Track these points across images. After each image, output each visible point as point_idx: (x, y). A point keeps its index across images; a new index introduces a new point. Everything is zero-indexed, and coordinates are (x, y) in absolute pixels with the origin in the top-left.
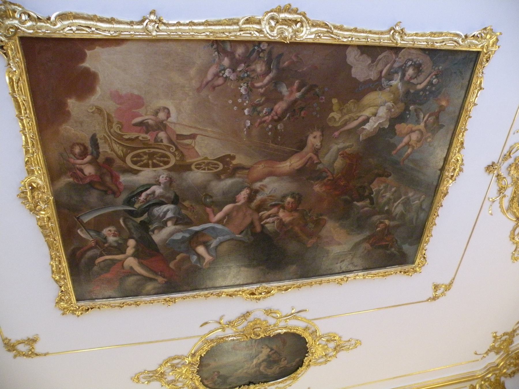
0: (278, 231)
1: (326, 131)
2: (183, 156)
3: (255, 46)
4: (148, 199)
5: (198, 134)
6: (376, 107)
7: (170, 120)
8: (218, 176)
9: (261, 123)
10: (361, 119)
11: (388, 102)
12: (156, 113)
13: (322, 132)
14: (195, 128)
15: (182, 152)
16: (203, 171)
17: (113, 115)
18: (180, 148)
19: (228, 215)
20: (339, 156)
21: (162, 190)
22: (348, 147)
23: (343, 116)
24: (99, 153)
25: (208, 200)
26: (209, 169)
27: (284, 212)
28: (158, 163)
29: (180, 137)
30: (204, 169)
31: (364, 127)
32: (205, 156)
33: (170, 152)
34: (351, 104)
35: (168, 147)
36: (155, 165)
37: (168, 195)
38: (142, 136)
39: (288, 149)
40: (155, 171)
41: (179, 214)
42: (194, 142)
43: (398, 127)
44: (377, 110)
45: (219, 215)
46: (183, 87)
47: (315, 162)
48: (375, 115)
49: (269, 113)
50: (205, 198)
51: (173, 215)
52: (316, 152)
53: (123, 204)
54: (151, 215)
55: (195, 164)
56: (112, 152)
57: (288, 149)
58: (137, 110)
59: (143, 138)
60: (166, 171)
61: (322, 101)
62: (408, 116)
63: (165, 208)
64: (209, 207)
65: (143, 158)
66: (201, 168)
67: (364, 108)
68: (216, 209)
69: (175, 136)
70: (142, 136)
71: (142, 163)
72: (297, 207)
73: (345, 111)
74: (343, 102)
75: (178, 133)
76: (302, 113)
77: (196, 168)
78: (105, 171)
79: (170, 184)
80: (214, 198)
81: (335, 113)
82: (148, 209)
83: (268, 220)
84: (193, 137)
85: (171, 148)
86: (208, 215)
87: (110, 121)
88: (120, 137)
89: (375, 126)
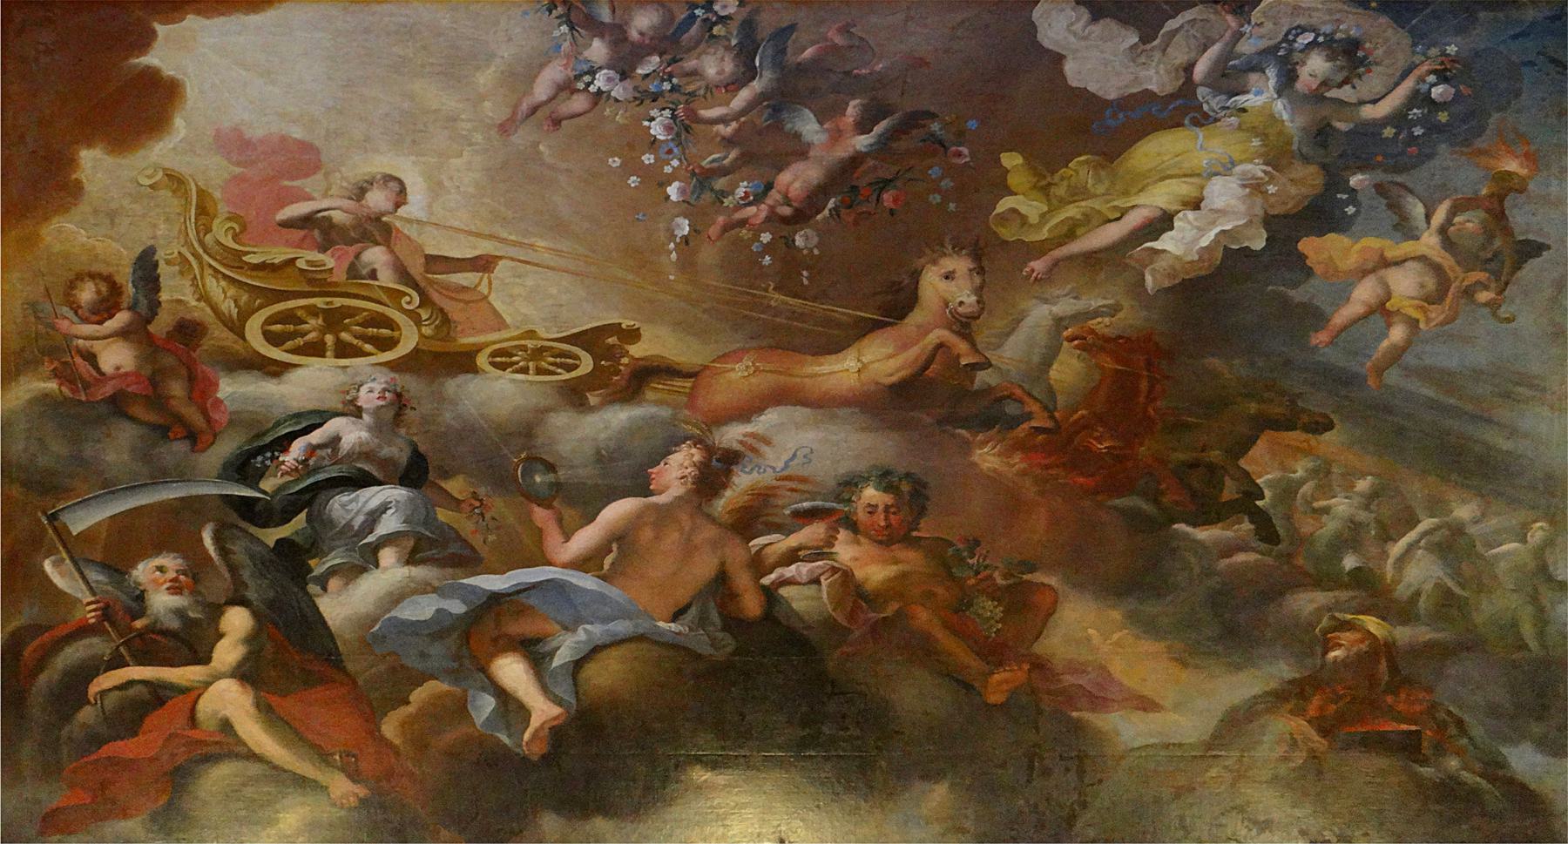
1: (992, 255)
4: (311, 462)
5: (501, 258)
7: (401, 211)
8: (575, 396)
9: (726, 228)
10: (1133, 220)
11: (1241, 162)
12: (360, 192)
13: (977, 256)
14: (491, 237)
15: (441, 310)
17: (217, 194)
18: (435, 297)
19: (621, 538)
21: (364, 435)
22: (1096, 313)
25: (538, 479)
26: (539, 371)
28: (355, 342)
29: (436, 262)
30: (525, 371)
32: (531, 327)
33: (404, 311)
34: (1080, 169)
35: (396, 295)
36: (344, 351)
37: (386, 452)
38: (307, 257)
39: (842, 313)
42: (485, 280)
44: (1202, 188)
45: (586, 538)
47: (964, 362)
48: (1196, 204)
52: (964, 325)
55: (488, 351)
57: (842, 313)
58: (296, 183)
60: (385, 370)
63: (373, 497)
64: (546, 503)
67: (1141, 182)
68: (569, 514)
70: (307, 257)
71: (300, 341)
73: (1061, 191)
74: (1046, 164)
76: (887, 197)
77: (494, 364)
78: (168, 360)
80: (562, 474)
81: (1020, 197)
84: (483, 264)
86: (539, 534)
87: (202, 211)
88: (234, 259)
89: (1204, 242)
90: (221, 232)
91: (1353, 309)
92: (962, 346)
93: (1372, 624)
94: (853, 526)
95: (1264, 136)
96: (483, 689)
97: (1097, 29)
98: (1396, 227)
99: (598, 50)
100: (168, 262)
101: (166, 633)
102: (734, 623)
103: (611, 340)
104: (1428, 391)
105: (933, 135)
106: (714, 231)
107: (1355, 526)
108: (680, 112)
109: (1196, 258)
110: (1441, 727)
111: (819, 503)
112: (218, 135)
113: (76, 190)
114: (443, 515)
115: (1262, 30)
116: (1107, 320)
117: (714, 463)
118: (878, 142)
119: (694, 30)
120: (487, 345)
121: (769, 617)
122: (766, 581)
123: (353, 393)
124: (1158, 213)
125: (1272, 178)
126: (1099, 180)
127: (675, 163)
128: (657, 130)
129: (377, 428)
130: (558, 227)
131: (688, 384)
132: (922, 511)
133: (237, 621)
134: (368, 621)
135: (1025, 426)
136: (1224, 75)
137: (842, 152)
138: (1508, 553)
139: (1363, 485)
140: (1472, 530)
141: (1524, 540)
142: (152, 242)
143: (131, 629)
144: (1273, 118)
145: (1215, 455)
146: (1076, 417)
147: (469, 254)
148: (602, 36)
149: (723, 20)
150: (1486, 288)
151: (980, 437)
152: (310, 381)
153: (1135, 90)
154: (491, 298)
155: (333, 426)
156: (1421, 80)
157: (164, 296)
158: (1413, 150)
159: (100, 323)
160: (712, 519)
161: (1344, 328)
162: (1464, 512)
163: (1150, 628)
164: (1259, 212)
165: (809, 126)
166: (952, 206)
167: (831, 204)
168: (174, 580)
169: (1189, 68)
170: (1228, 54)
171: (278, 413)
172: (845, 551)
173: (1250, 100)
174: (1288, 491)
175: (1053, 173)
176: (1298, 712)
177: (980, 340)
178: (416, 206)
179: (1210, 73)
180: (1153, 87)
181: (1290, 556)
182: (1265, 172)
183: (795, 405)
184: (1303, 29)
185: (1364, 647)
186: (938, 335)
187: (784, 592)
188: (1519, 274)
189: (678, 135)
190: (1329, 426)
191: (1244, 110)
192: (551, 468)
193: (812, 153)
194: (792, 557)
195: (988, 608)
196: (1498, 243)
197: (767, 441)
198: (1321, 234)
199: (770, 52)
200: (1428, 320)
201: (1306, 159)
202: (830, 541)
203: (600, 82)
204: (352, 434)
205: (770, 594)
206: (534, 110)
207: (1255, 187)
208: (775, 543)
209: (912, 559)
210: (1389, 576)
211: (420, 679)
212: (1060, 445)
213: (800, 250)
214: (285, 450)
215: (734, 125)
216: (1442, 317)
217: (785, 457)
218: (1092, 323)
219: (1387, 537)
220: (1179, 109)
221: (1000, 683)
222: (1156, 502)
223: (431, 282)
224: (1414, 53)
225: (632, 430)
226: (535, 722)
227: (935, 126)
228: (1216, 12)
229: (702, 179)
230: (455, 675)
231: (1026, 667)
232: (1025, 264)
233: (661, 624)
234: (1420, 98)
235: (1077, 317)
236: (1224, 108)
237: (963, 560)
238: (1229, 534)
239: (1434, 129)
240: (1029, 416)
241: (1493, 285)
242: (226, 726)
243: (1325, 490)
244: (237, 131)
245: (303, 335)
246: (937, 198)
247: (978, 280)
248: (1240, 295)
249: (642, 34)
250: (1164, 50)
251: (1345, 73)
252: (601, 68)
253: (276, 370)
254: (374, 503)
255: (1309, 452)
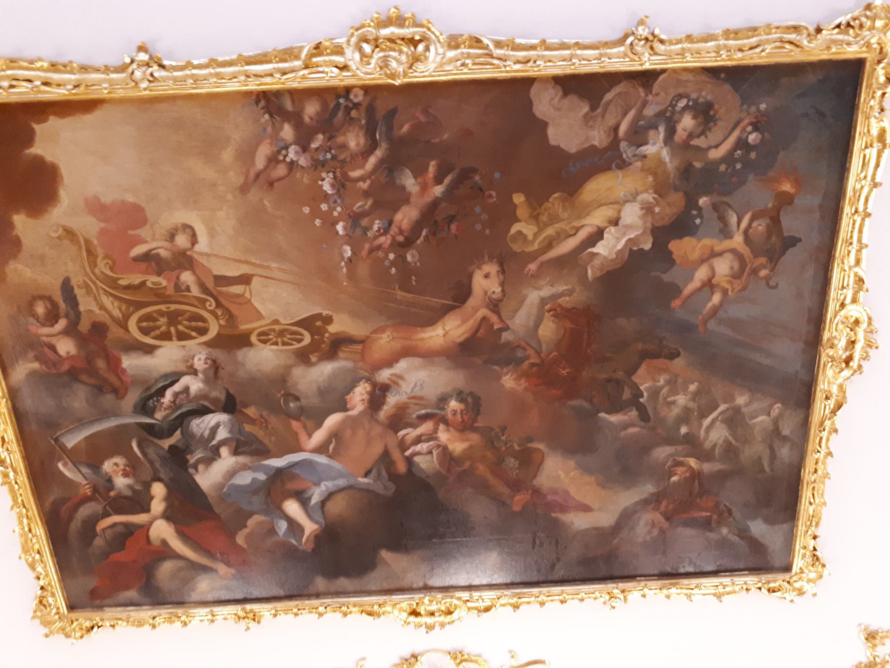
0: (444, 472)
2: (231, 318)
3: (338, 97)
4: (177, 402)
5: (253, 275)
6: (616, 206)
7: (197, 248)
8: (303, 357)
9: (371, 251)
10: (582, 234)
11: (642, 192)
12: (172, 237)
13: (501, 264)
15: (227, 309)
16: (275, 347)
17: (95, 242)
19: (335, 435)
20: (547, 314)
21: (201, 385)
22: (562, 295)
23: (540, 230)
24: (80, 313)
25: (292, 405)
26: (284, 344)
27: (448, 430)
28: (186, 330)
29: (221, 280)
30: (276, 344)
31: (594, 250)
32: (276, 317)
36: (182, 337)
37: (215, 394)
38: (152, 280)
39: (435, 301)
40: (184, 347)
41: (240, 432)
43: (675, 246)
44: (619, 211)
45: (319, 436)
46: (214, 185)
47: (495, 327)
48: (615, 222)
49: (386, 231)
50: (286, 403)
51: (228, 435)
52: (495, 306)
53: (133, 412)
54: (188, 436)
55: (256, 332)
56: (103, 312)
57: (435, 301)
58: (137, 232)
59: (153, 283)
60: (205, 347)
61: (491, 201)
62: (698, 221)
63: (212, 419)
64: (297, 419)
65: (158, 323)
66: (269, 340)
67: (586, 210)
68: (310, 424)
69: (212, 279)
70: (152, 280)
71: (158, 332)
72: (475, 421)
73: (544, 218)
74: (537, 201)
75: (216, 272)
76: (453, 227)
77: (260, 341)
78: (93, 347)
79: (216, 373)
80: (304, 402)
81: (523, 223)
82: (181, 421)
83: (418, 448)
84: (245, 280)
85: (208, 303)
87: (89, 252)
88: (113, 283)
89: (619, 247)
90: (102, 266)
91: (695, 284)
92: (494, 318)
93: (693, 462)
94: (446, 422)
95: (655, 174)
96: (281, 518)
97: (566, 101)
98: (721, 231)
99: (287, 132)
100: (79, 287)
101: (126, 497)
102: (393, 477)
103: (318, 323)
104: (728, 332)
105: (476, 183)
106: (364, 253)
107: (687, 410)
108: (338, 174)
109: (614, 256)
110: (721, 515)
111: (429, 411)
112: (86, 201)
113: (17, 243)
114: (248, 428)
115: (659, 99)
116: (567, 298)
117: (377, 391)
118: (447, 190)
119: (340, 114)
120: (254, 329)
121: (410, 471)
122: (407, 453)
123: (191, 361)
124: (595, 229)
125: (657, 202)
126: (565, 209)
127: (339, 209)
128: (327, 187)
129: (206, 381)
130: (281, 255)
131: (359, 347)
132: (478, 413)
133: (158, 490)
134: (220, 486)
135: (527, 363)
136: (636, 132)
137: (428, 199)
138: (761, 422)
139: (693, 387)
140: (744, 410)
141: (769, 414)
142: (67, 275)
143: (109, 497)
144: (661, 162)
145: (620, 374)
146: (552, 356)
147: (236, 273)
148: (289, 121)
149: (356, 106)
150: (765, 267)
151: (505, 370)
152: (167, 356)
153: (586, 145)
154: (252, 301)
155: (185, 380)
156: (744, 129)
157: (82, 308)
158: (735, 179)
159: (52, 326)
160: (377, 421)
161: (689, 297)
162: (741, 400)
163: (587, 470)
164: (649, 225)
165: (409, 182)
166: (487, 231)
167: (424, 233)
168: (124, 470)
169: (616, 129)
170: (639, 116)
171: (155, 375)
172: (443, 436)
173: (649, 149)
174: (655, 393)
175: (540, 205)
176: (656, 509)
177: (503, 314)
178: (203, 245)
179: (627, 132)
180: (596, 143)
181: (655, 428)
182: (654, 198)
183: (413, 356)
184: (680, 96)
185: (688, 475)
186: (483, 312)
187: (417, 459)
188: (783, 258)
189: (338, 190)
190: (678, 355)
191: (645, 156)
192: (297, 399)
193: (412, 200)
194: (418, 440)
195: (511, 462)
196: (774, 238)
197: (401, 377)
198: (681, 237)
199: (384, 129)
200: (733, 290)
201: (676, 189)
202: (436, 431)
203: (292, 155)
204: (195, 385)
205: (409, 460)
206: (258, 176)
207: (648, 209)
208: (409, 433)
209: (475, 438)
210: (702, 437)
211: (250, 515)
212: (543, 375)
213: (410, 264)
214: (163, 396)
215: (368, 182)
216: (740, 287)
217: (411, 386)
218: (560, 301)
219: (703, 416)
220: (607, 159)
221: (519, 501)
222: (591, 402)
223: (220, 292)
224: (741, 112)
225: (334, 376)
226: (307, 532)
227: (477, 178)
228: (634, 87)
229: (354, 219)
230: (266, 512)
231: (530, 492)
232: (525, 267)
233: (360, 479)
234: (742, 144)
235: (554, 297)
236: (634, 156)
237: (499, 438)
238: (626, 418)
239: (748, 165)
240: (528, 358)
241: (768, 266)
242: (164, 542)
243: (674, 392)
244: (96, 198)
245: (159, 328)
246: (478, 227)
247: (501, 277)
248: (640, 278)
249: (311, 118)
250: (603, 116)
251: (702, 127)
252: (291, 145)
253: (149, 350)
254: (213, 423)
255: (666, 370)
